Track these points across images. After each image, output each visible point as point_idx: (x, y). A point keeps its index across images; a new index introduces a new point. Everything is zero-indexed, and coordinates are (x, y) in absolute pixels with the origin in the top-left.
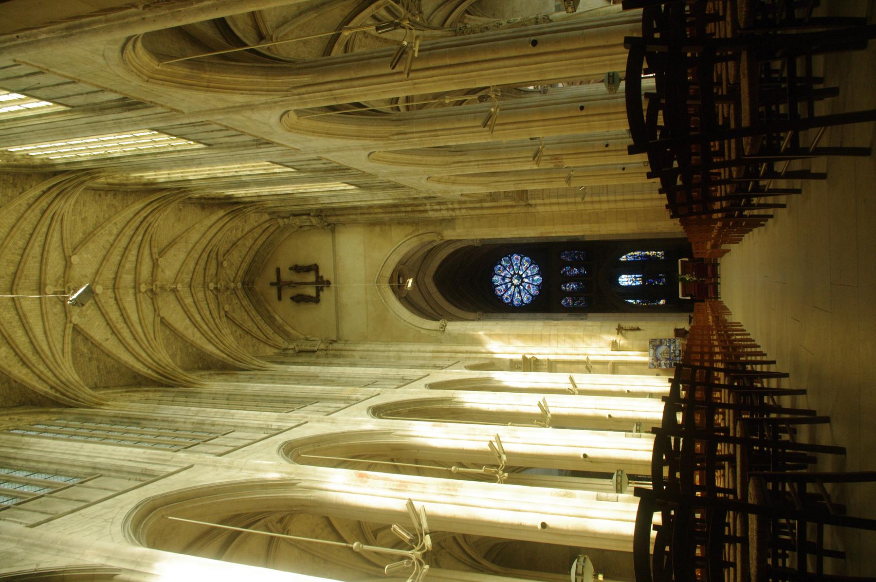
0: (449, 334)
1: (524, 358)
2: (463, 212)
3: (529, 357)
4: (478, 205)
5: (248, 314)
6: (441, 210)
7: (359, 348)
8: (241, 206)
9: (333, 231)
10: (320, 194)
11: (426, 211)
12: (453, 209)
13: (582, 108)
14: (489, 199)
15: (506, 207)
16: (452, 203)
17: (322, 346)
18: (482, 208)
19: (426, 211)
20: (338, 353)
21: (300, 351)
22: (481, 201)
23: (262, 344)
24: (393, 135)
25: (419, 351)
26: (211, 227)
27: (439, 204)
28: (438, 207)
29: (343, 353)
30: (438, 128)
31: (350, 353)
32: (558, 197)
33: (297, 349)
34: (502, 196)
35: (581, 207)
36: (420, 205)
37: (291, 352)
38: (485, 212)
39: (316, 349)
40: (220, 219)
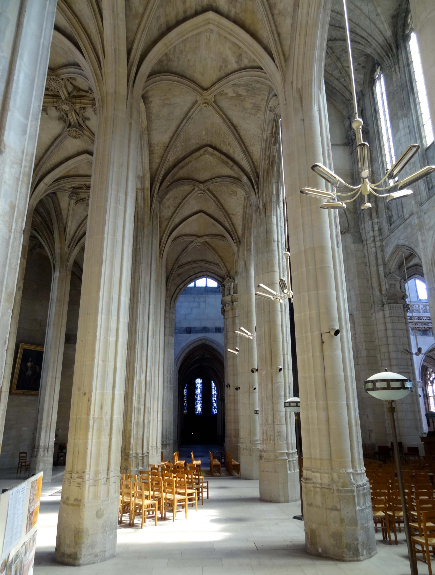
2: (374, 249)
4: (380, 261)
6: (373, 231)
8: (395, 51)
9: (345, 145)
10: (414, 116)
11: (371, 218)
12: (374, 241)
14: (387, 271)
15: (380, 285)
16: (382, 240)
18: (377, 265)
19: (371, 218)
22: (385, 265)
26: (375, 24)
27: (380, 230)
28: (376, 228)
32: (393, 330)
34: (390, 282)
35: (384, 349)
36: (377, 214)
38: (373, 268)
40: (381, 33)
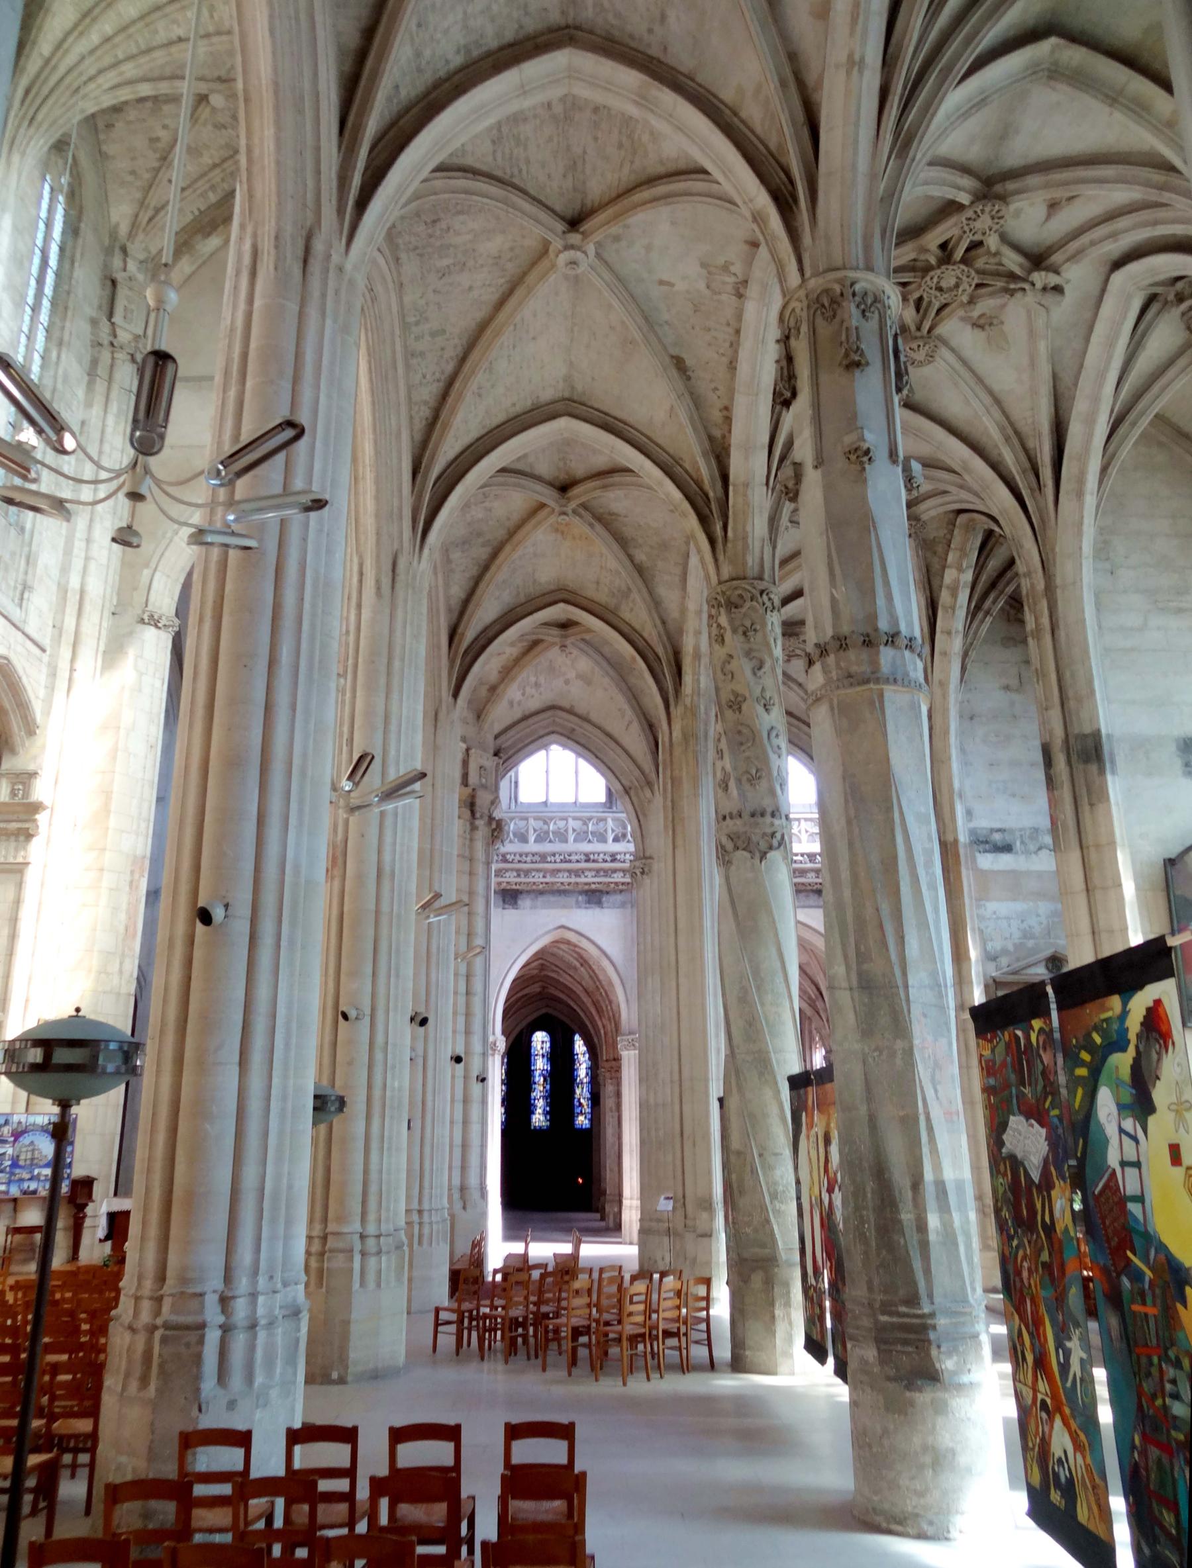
0: (131, 633)
1: (36, 807)
3: (41, 818)
5: (215, 166)
7: (110, 421)
13: (205, 917)
17: (124, 336)
20: (102, 370)
21: (114, 283)
23: (138, 195)
24: (255, 235)
25: (87, 559)
29: (100, 386)
30: (249, 384)
31: (99, 399)
33: (120, 276)
37: (117, 262)
39: (117, 319)
